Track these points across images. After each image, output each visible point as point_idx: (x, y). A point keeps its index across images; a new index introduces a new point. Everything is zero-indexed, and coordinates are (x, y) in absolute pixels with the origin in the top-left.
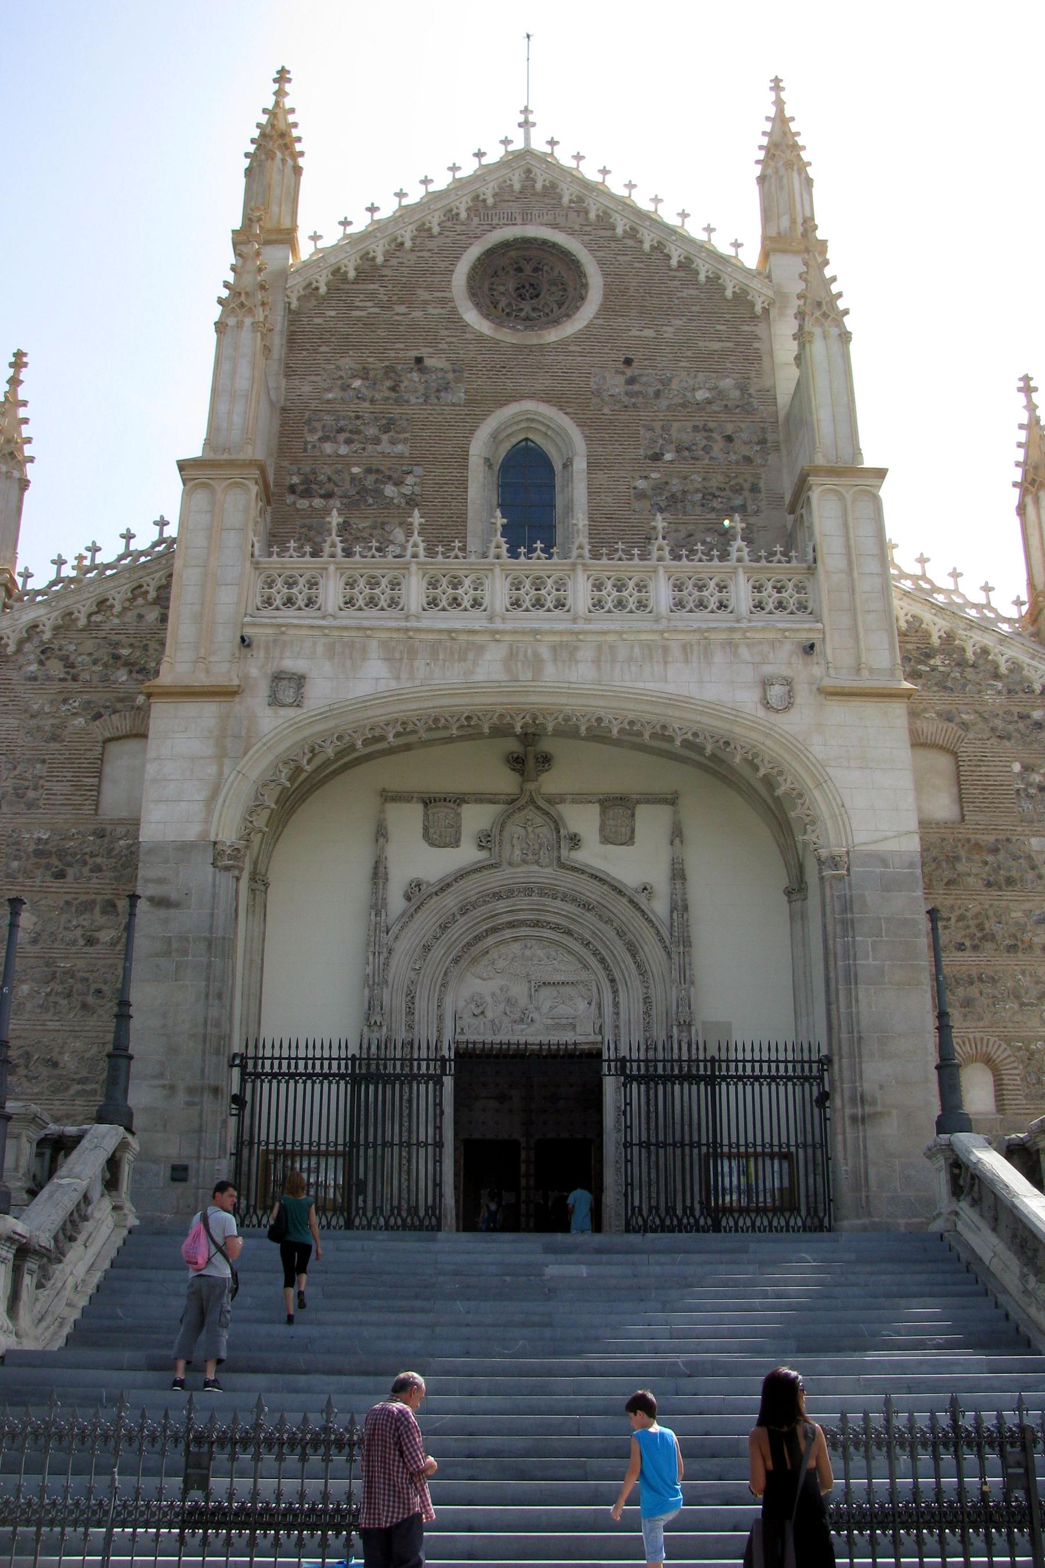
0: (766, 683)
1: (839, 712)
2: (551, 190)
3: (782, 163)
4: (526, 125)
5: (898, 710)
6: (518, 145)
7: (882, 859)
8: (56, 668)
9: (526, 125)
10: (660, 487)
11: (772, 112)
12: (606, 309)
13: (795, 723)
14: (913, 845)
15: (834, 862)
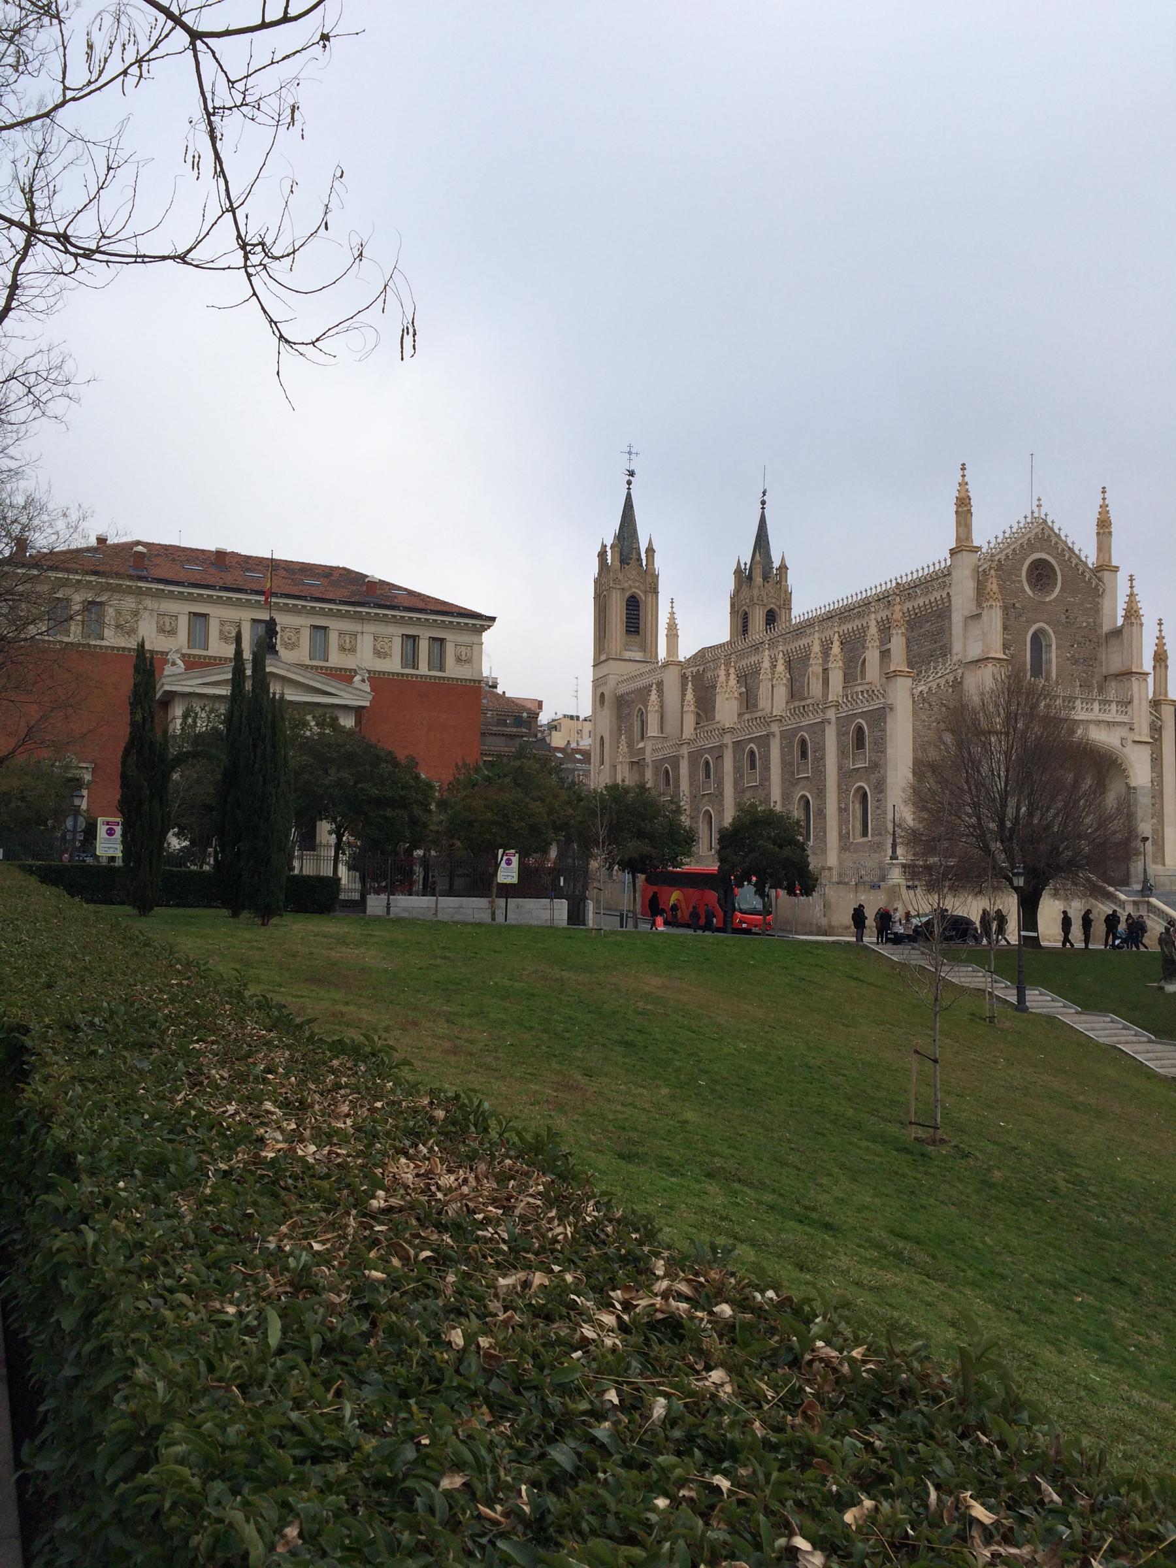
0: (1122, 739)
1: (1137, 747)
2: (1049, 539)
3: (1104, 525)
4: (1039, 506)
5: (1148, 747)
6: (1036, 515)
7: (1143, 788)
8: (926, 705)
9: (1039, 506)
10: (1073, 656)
11: (1101, 502)
12: (1062, 590)
13: (1125, 750)
14: (1150, 785)
15: (1134, 788)
